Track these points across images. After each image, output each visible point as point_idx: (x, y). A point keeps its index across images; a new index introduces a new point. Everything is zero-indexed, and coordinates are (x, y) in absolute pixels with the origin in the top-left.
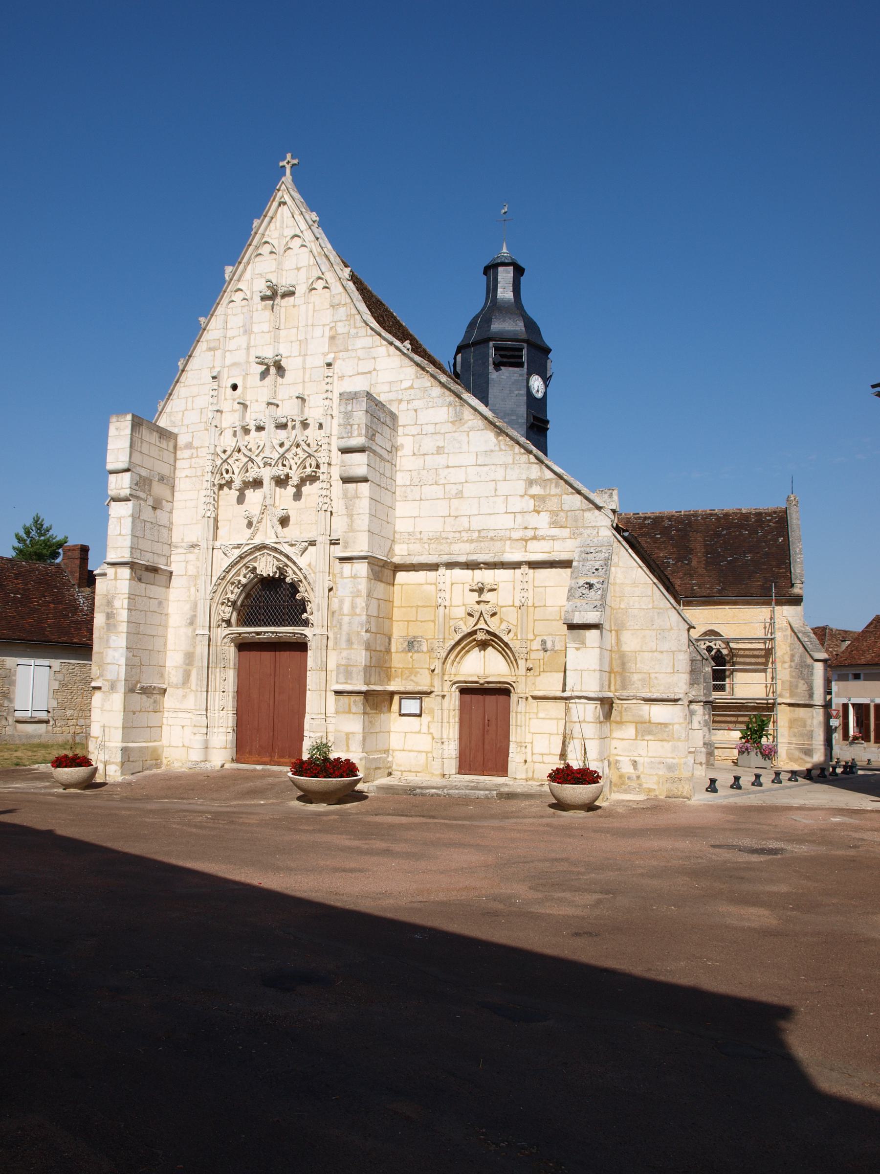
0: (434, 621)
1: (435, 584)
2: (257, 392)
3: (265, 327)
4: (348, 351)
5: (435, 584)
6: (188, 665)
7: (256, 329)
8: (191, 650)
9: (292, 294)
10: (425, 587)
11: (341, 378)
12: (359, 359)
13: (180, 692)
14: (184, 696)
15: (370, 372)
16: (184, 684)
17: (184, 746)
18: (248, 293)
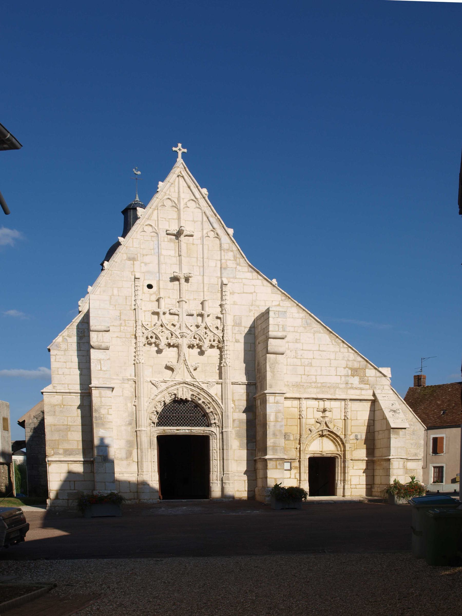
0: (297, 426)
1: (297, 408)
2: (169, 293)
3: (172, 253)
4: (236, 278)
5: (297, 408)
6: (130, 447)
7: (164, 252)
8: (132, 439)
9: (192, 236)
10: (292, 409)
11: (232, 293)
12: (244, 284)
13: (125, 463)
14: (129, 465)
15: (252, 293)
16: (127, 458)
17: (131, 492)
18: (157, 229)
